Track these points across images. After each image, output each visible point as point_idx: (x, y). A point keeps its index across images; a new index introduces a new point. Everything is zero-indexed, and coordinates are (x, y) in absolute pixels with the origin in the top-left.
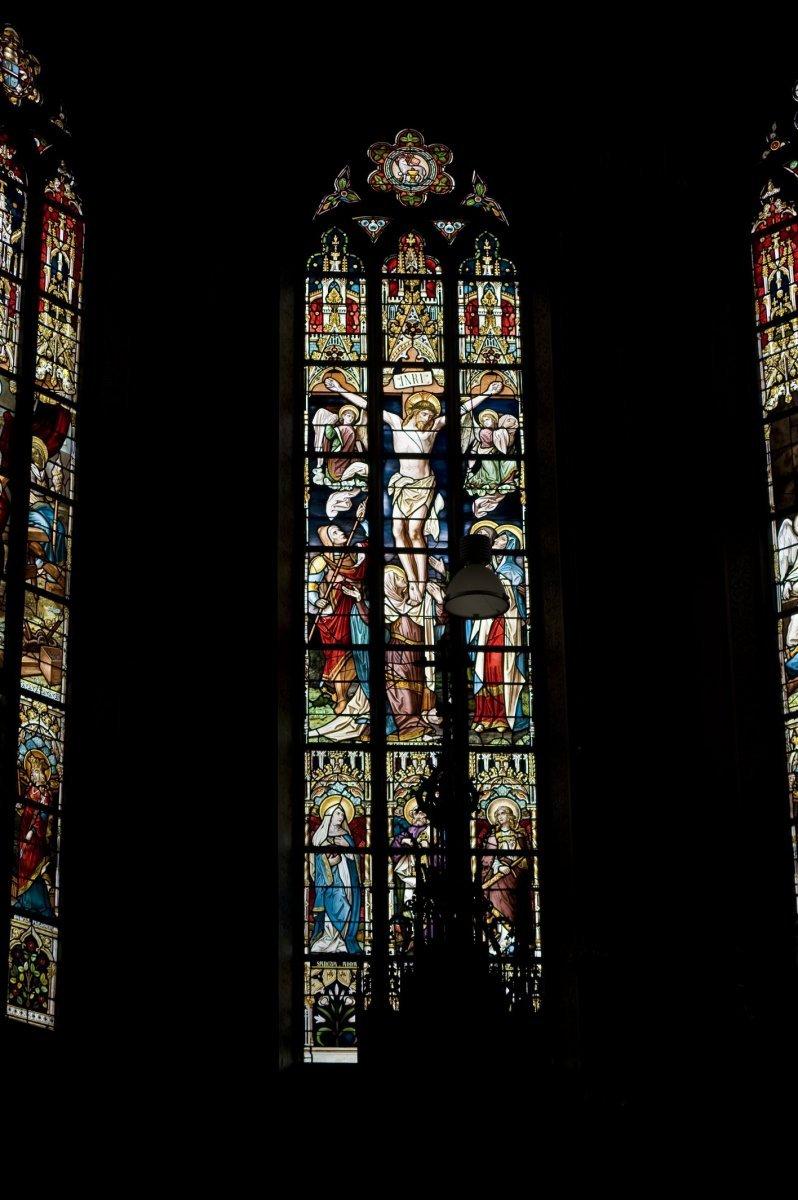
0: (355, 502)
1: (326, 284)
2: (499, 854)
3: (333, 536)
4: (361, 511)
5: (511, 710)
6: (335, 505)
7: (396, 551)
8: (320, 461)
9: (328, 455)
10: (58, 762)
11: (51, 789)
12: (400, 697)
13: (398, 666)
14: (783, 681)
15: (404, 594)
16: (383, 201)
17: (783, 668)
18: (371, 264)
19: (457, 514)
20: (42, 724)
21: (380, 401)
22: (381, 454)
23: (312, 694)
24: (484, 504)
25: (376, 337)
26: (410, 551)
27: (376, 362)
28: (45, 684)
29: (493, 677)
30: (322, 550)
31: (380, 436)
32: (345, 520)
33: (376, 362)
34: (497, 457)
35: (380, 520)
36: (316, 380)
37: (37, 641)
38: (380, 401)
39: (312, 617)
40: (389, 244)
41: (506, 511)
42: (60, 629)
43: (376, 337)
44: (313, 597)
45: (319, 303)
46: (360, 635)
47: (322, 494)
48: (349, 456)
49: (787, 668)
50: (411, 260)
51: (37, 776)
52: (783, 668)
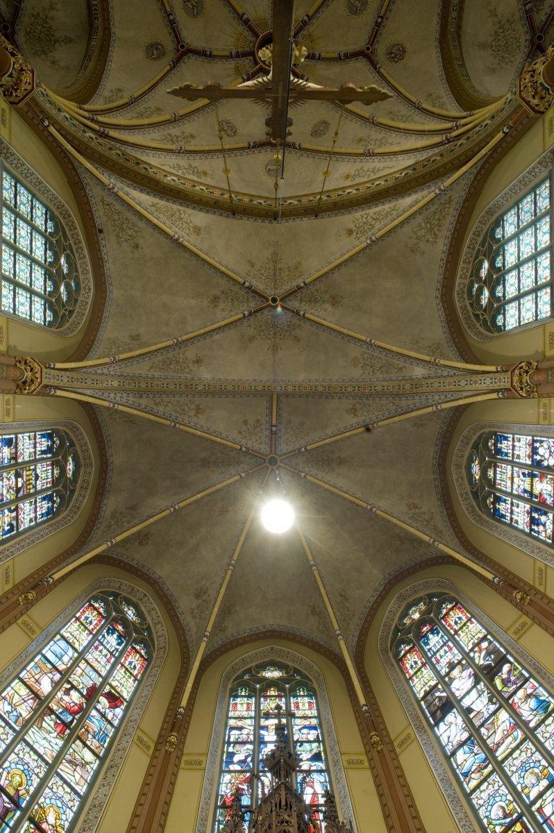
4: (249, 759)
8: (232, 745)
10: (67, 820)
11: (56, 830)
14: (462, 780)
17: (460, 775)
20: (64, 796)
28: (74, 781)
30: (230, 772)
32: (241, 762)
37: (77, 763)
39: (222, 796)
42: (92, 765)
44: (224, 789)
45: (236, 704)
49: (462, 774)
51: (51, 819)
52: (460, 775)
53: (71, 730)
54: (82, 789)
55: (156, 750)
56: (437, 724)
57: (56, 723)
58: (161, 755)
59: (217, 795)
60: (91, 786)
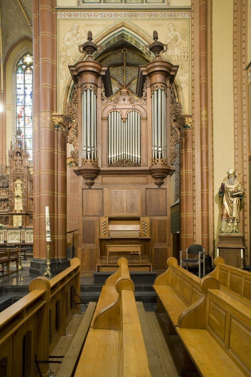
1: (19, 74)
6: (20, 101)
7: (26, 106)
9: (19, 95)
12: (27, 122)
13: (26, 118)
15: (27, 111)
16: (25, 64)
18: (24, 71)
21: (25, 88)
22: (25, 95)
25: (24, 80)
26: (28, 106)
27: (25, 84)
31: (25, 92)
32: (21, 102)
33: (25, 84)
35: (25, 102)
36: (18, 86)
38: (25, 88)
40: (26, 69)
43: (24, 80)
46: (23, 115)
47: (19, 99)
48: (22, 95)
50: (28, 71)
59: (16, 114)
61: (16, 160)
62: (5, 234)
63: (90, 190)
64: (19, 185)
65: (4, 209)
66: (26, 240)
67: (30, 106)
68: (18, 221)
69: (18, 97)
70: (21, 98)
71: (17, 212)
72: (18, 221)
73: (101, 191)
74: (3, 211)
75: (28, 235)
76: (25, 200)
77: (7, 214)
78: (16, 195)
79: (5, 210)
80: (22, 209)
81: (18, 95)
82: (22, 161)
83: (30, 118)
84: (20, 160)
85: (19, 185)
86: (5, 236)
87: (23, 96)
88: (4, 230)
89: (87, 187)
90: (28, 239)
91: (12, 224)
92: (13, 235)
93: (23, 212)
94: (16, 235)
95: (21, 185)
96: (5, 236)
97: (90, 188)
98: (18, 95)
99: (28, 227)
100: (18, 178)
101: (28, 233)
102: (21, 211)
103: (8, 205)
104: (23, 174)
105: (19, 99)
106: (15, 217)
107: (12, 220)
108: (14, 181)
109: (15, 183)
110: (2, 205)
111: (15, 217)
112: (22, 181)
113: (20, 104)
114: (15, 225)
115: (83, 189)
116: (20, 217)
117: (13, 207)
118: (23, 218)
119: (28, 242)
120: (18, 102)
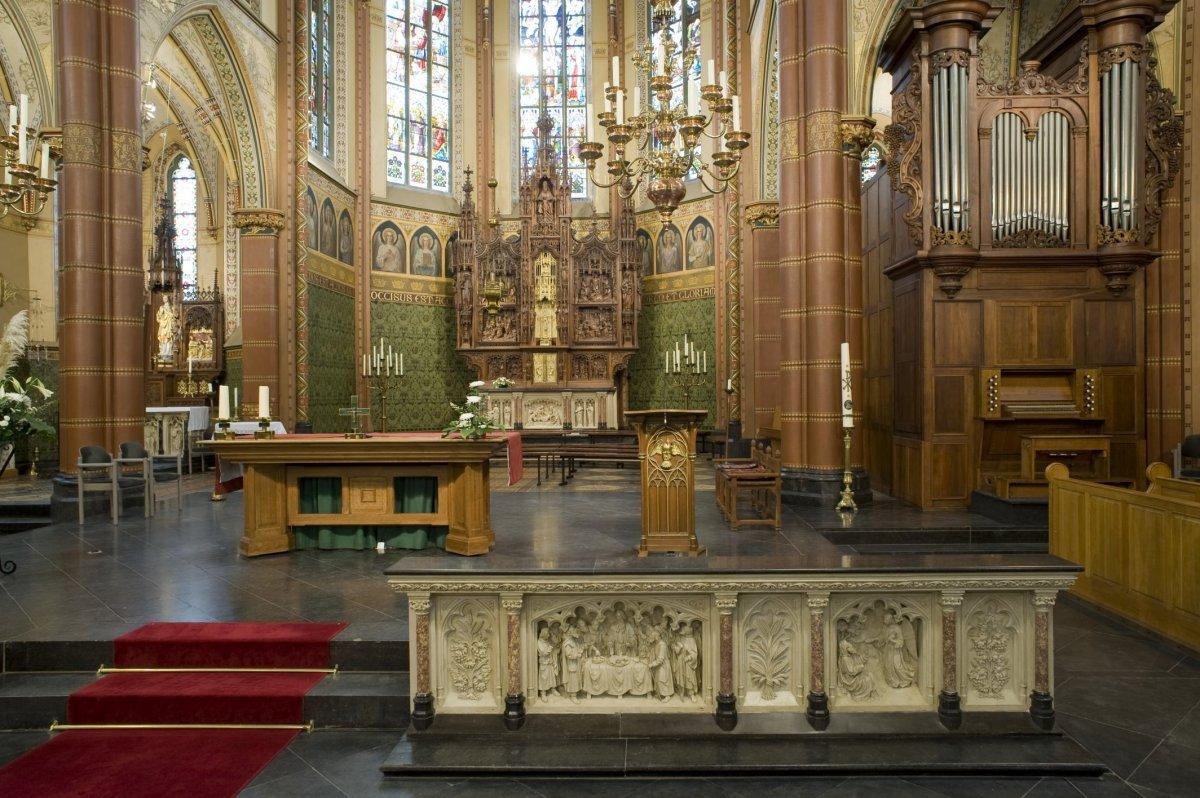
0: (535, 31)
2: (575, 137)
3: (528, 42)
5: (579, 94)
6: (529, 32)
15: (548, 60)
19: (565, 35)
22: (542, 16)
23: (522, 92)
24: (573, 30)
29: (574, 85)
32: (532, 36)
34: (577, 15)
35: (542, 36)
41: (580, 32)
47: (525, 29)
53: (427, 62)
54: (446, 95)
55: (478, 52)
56: (654, 33)
57: (419, 63)
58: (481, 56)
60: (450, 89)
61: (538, 202)
62: (516, 406)
63: (952, 305)
64: (546, 270)
65: (501, 336)
66: (573, 422)
67: (556, 46)
68: (545, 368)
69: (523, 23)
70: (532, 25)
71: (543, 344)
72: (545, 368)
73: (977, 306)
74: (501, 340)
75: (579, 408)
76: (566, 311)
77: (512, 350)
78: (541, 298)
79: (506, 338)
80: (555, 335)
81: (522, 17)
82: (554, 203)
83: (556, 80)
84: (550, 201)
85: (546, 270)
86: (518, 411)
87: (537, 20)
88: (515, 394)
89: (945, 298)
90: (580, 419)
91: (530, 378)
92: (538, 409)
93: (558, 345)
94: (547, 409)
95: (553, 267)
96: (518, 411)
97: (951, 300)
98: (522, 17)
99: (574, 384)
100: (546, 249)
101: (579, 402)
102: (553, 343)
103: (513, 326)
104: (559, 239)
105: (525, 29)
106: (538, 358)
107: (532, 367)
108: (535, 258)
109: (537, 262)
110: (498, 325)
111: (538, 358)
112: (556, 258)
113: (528, 42)
114: (538, 379)
115: (934, 301)
116: (552, 358)
117: (532, 330)
118: (559, 361)
119: (580, 426)
120: (525, 38)
